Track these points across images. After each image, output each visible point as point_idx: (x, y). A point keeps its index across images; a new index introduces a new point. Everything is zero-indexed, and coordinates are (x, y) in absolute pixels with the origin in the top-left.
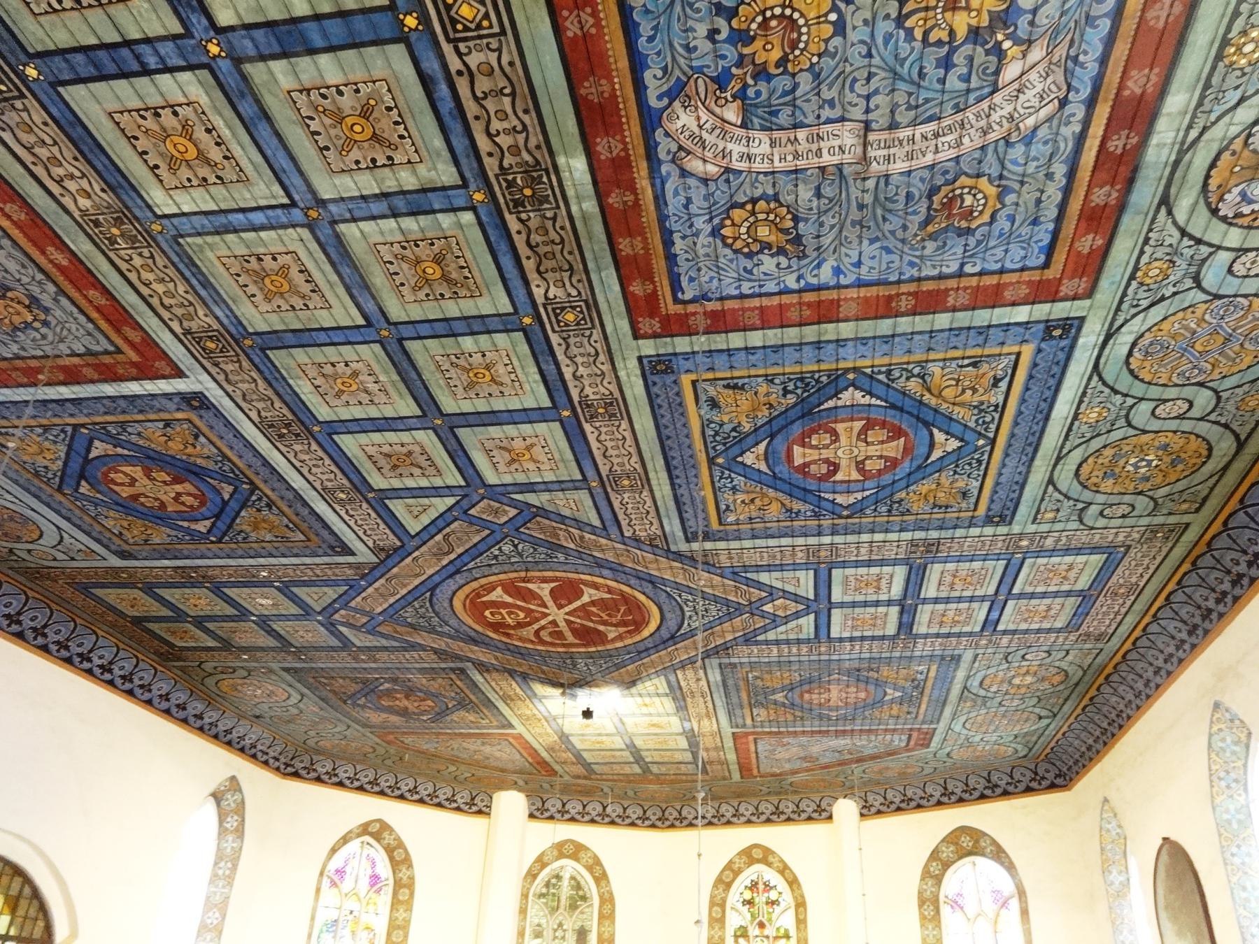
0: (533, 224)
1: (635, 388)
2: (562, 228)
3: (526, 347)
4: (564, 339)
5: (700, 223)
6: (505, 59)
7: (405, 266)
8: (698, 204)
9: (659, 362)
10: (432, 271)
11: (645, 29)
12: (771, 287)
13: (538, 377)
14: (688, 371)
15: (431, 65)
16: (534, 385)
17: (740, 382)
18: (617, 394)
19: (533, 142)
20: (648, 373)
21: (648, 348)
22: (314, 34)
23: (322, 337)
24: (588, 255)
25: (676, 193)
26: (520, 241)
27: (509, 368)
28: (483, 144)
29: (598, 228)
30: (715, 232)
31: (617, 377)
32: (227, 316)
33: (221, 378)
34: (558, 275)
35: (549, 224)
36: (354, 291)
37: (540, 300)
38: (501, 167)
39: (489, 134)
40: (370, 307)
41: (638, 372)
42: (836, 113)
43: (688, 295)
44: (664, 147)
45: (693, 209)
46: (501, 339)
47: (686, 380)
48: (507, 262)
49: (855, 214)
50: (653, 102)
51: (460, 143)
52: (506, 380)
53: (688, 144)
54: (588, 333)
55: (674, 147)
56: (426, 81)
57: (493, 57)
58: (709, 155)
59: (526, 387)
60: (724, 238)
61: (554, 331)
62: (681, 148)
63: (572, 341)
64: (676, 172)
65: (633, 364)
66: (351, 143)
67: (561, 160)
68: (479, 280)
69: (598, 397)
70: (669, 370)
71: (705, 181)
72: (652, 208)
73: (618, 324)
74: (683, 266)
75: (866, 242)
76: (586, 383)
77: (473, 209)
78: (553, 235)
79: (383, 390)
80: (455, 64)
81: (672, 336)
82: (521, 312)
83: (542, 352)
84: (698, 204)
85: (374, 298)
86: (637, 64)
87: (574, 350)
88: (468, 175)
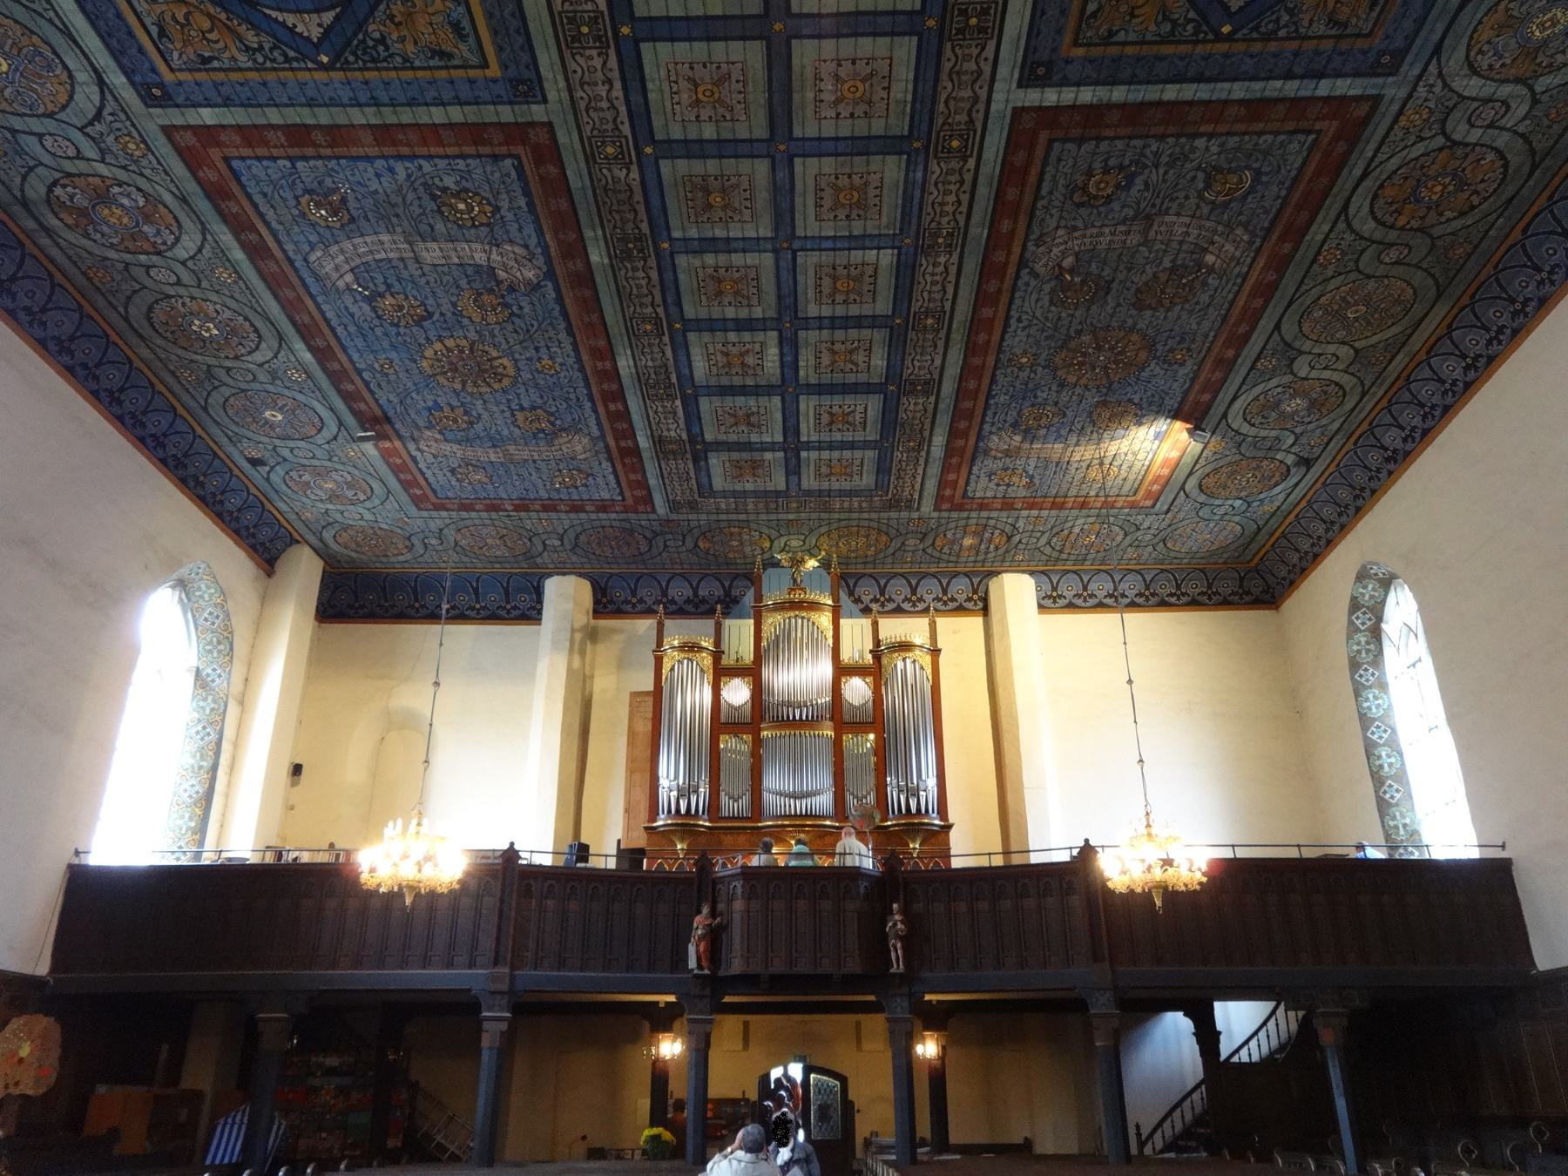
0: (631, 225)
1: (547, 60)
2: (609, 221)
3: (655, 123)
4: (617, 128)
5: (509, 216)
6: (632, 309)
7: (736, 205)
8: (514, 228)
9: (526, 94)
10: (716, 199)
11: (556, 313)
12: (442, 163)
13: (650, 86)
14: (495, 81)
15: (673, 310)
16: (655, 76)
17: (435, 62)
18: (567, 55)
19: (623, 272)
20: (536, 83)
21: (538, 112)
22: (730, 325)
23: (841, 147)
24: (592, 200)
25: (529, 236)
26: (643, 215)
27: (676, 98)
28: (654, 275)
29: (583, 219)
30: (497, 209)
31: (567, 79)
32: (914, 171)
33: (981, 106)
34: (617, 187)
35: (619, 224)
36: (787, 187)
37: (634, 168)
38: (645, 262)
39: (649, 278)
40: (782, 174)
41: (546, 85)
42: (439, 269)
43: (508, 162)
44: (540, 261)
45: (516, 226)
46: (677, 134)
47: (494, 70)
48: (655, 201)
49: (400, 211)
50: (550, 285)
51: (669, 276)
52: (684, 84)
53: (526, 262)
54: (595, 133)
55: (534, 261)
56: (679, 304)
57: (638, 310)
58: (511, 255)
59: (663, 73)
60: (489, 204)
61: (626, 137)
62: (530, 261)
63: (610, 126)
64: (531, 248)
65: (552, 95)
66: (735, 282)
67: (606, 261)
68: (681, 189)
69: (588, 52)
70: (515, 82)
71: (511, 242)
72: (545, 228)
73: (566, 137)
74: (517, 186)
75: (381, 190)
76: (599, 74)
77: (671, 239)
78: (617, 217)
79: (818, 78)
80: (660, 310)
81: (517, 124)
82: (652, 159)
83: (640, 115)
84: (514, 228)
85: (775, 183)
86: (560, 299)
87: (609, 115)
88: (668, 260)
